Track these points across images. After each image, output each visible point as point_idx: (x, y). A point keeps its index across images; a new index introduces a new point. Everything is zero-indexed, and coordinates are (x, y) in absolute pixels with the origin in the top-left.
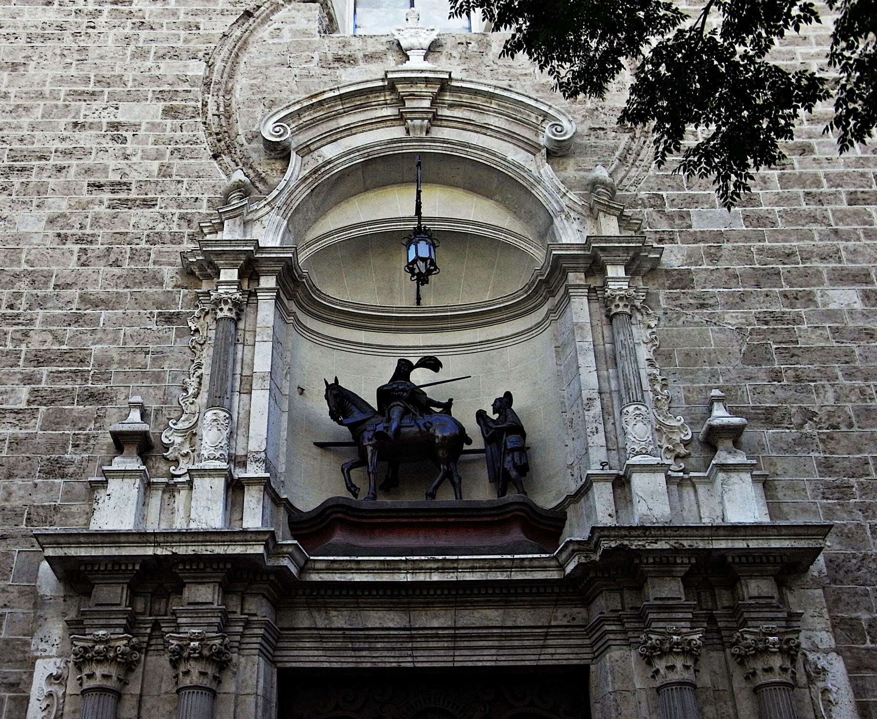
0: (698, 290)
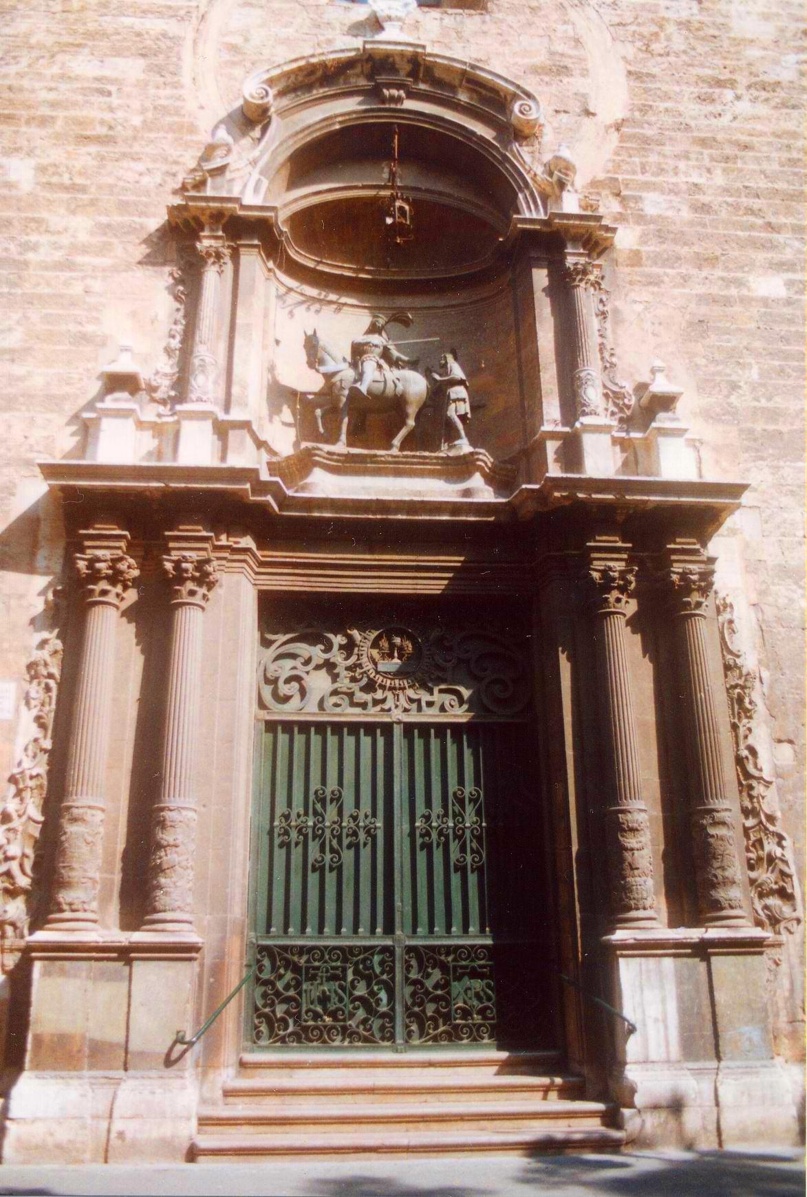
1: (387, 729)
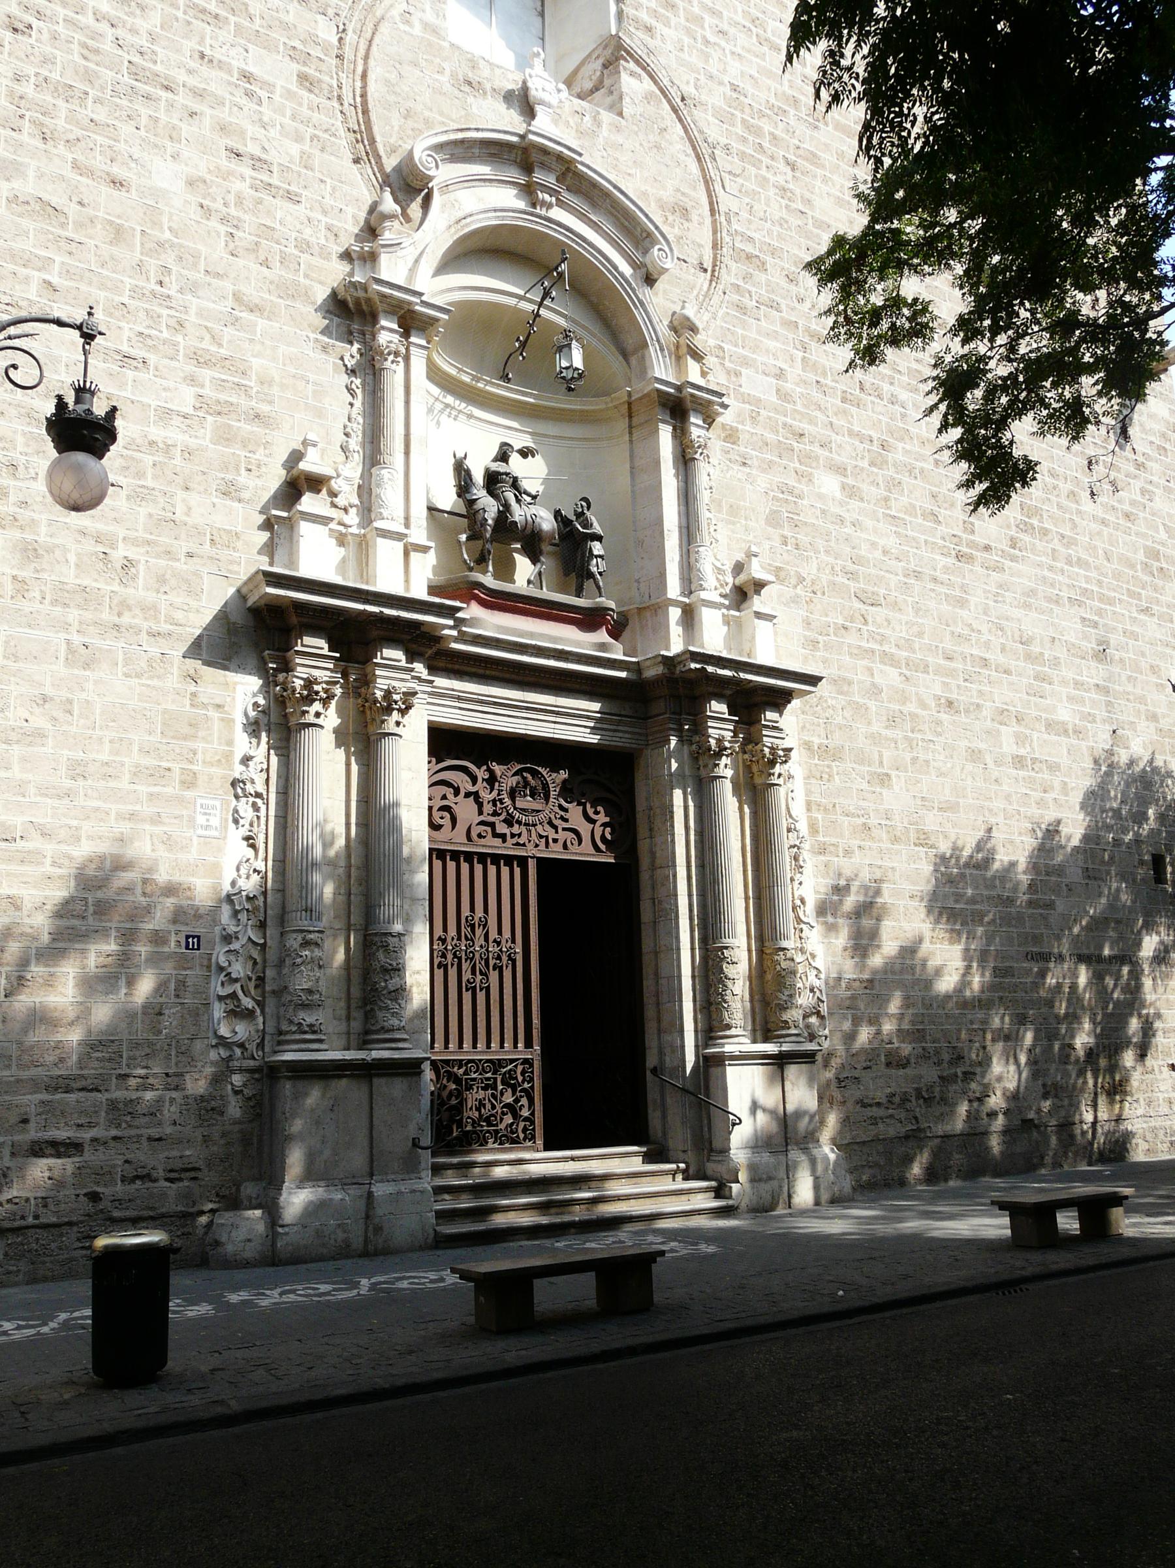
0: (742, 449)
1: (523, 861)
